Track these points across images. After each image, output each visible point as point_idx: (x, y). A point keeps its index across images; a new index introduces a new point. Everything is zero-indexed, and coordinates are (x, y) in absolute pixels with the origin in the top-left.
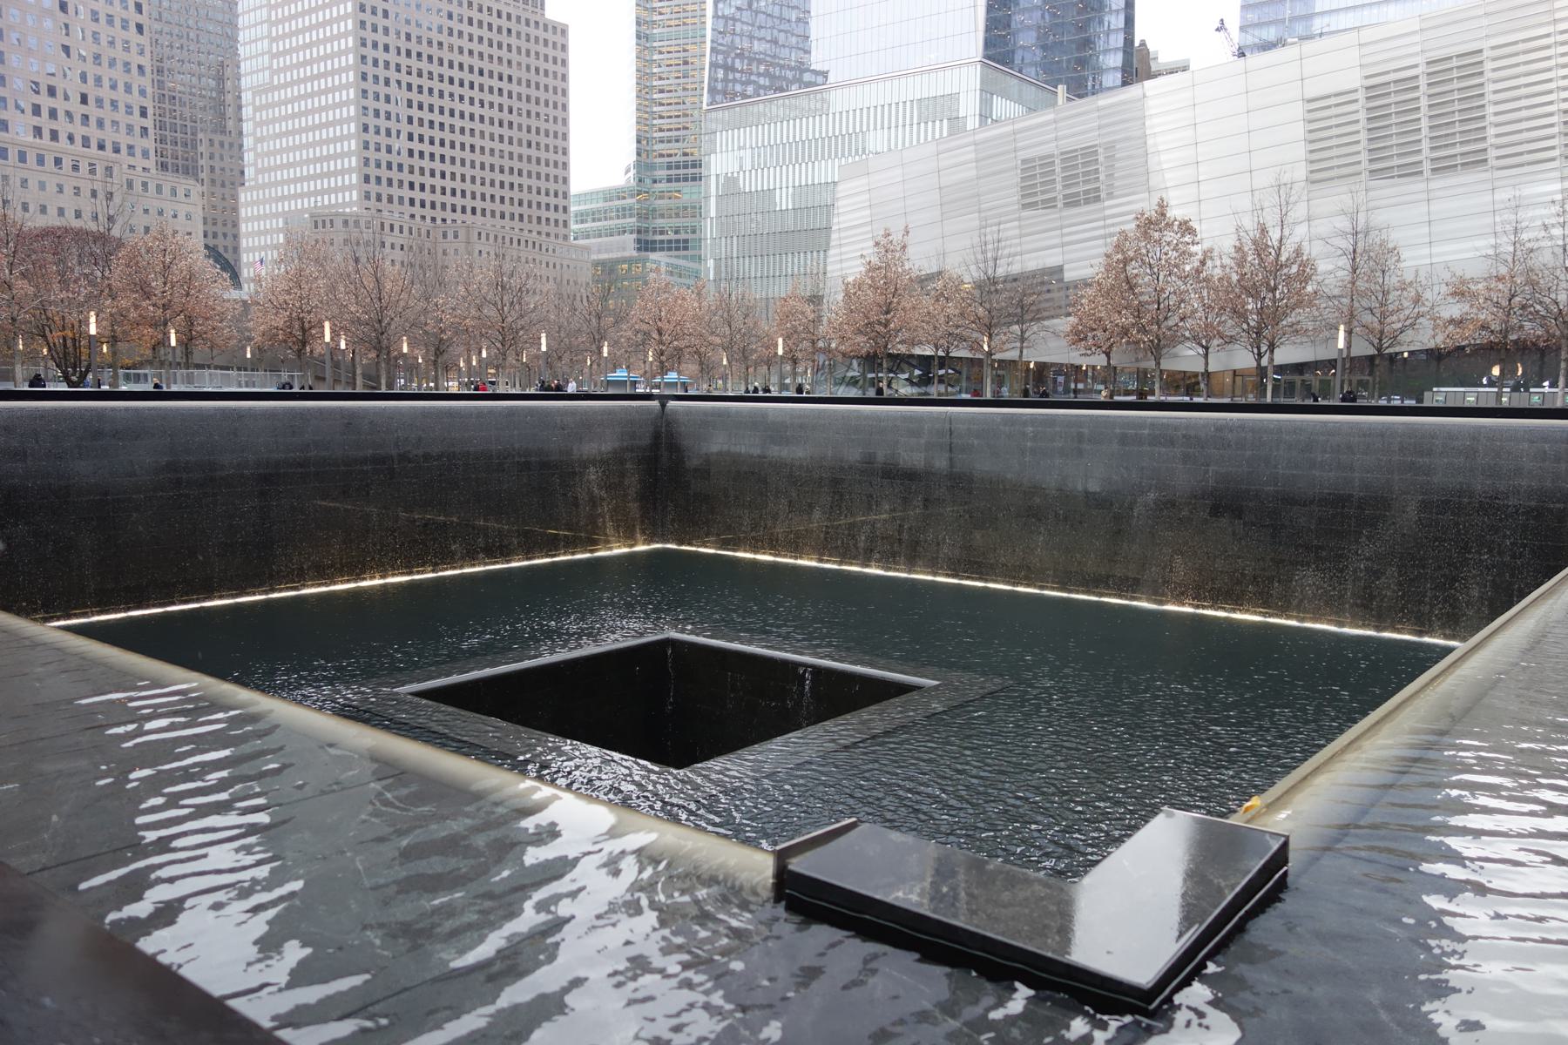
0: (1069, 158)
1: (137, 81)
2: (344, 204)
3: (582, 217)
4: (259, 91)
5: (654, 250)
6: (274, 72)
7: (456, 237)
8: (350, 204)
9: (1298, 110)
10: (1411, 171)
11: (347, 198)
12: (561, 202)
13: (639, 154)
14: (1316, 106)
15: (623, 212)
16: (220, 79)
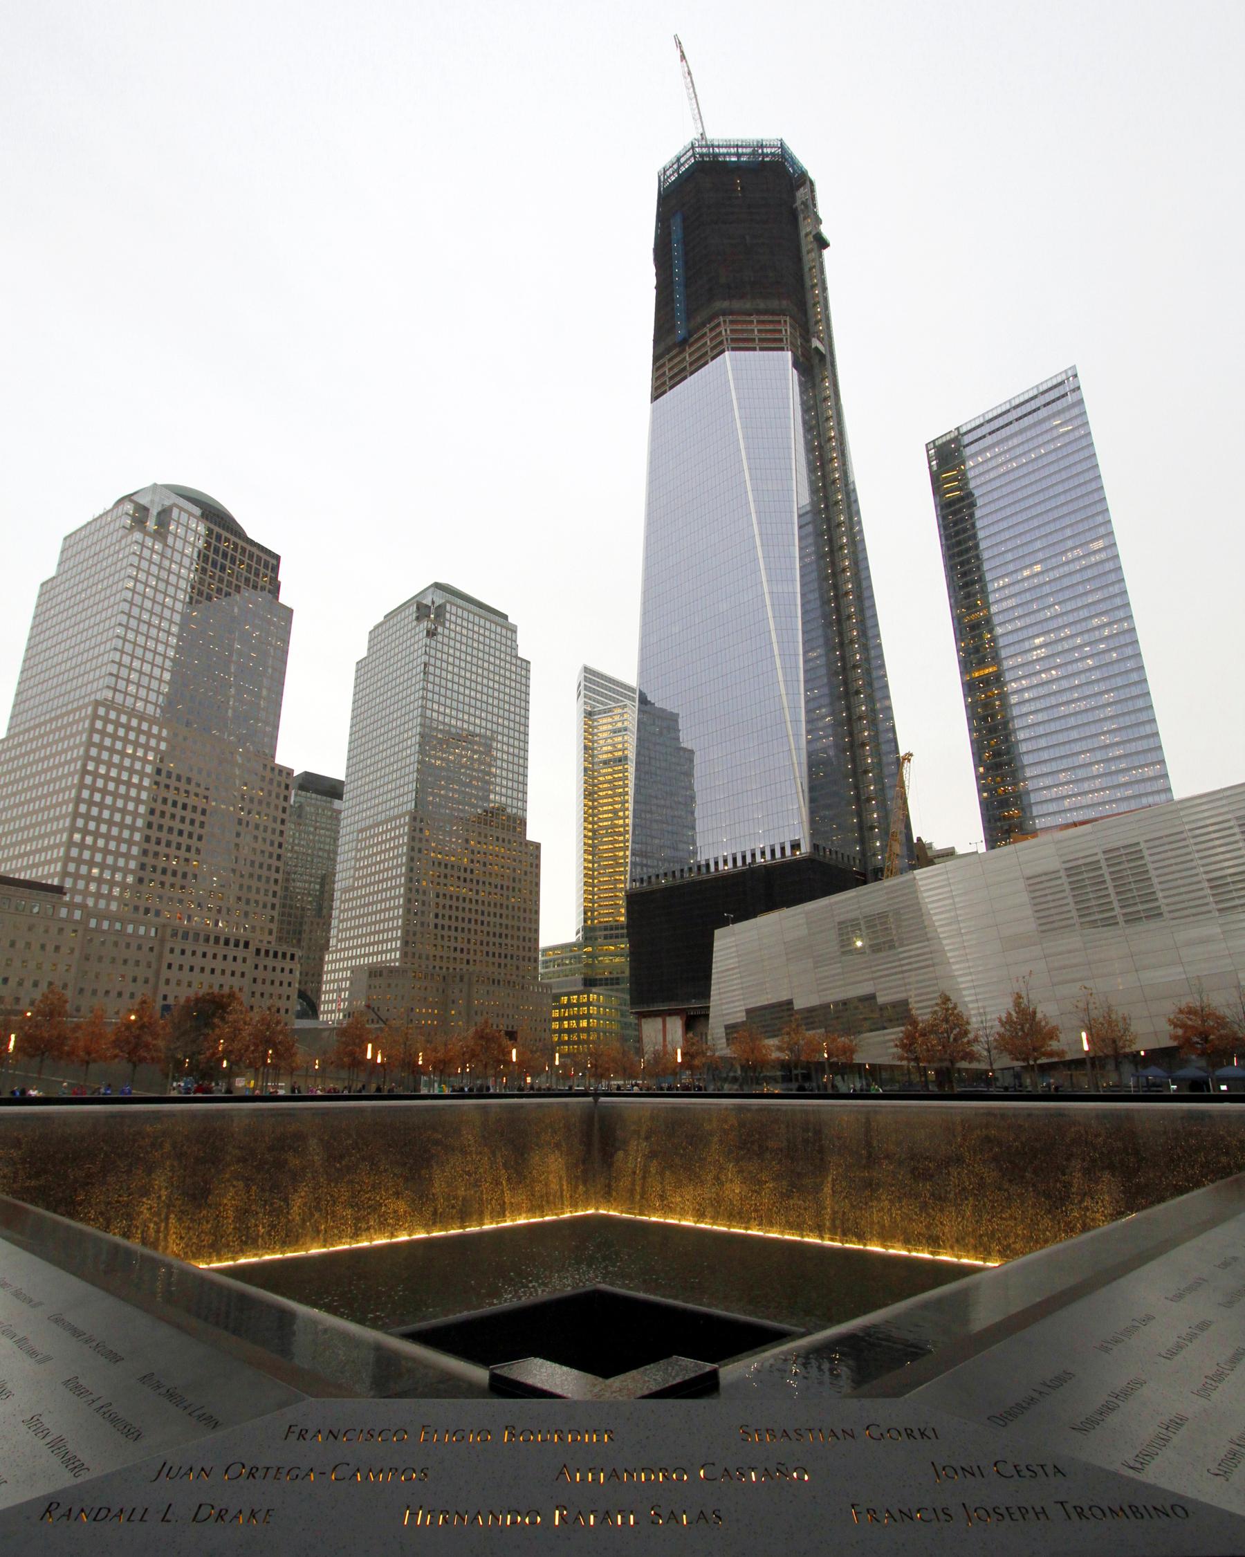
2: (391, 961)
4: (345, 891)
5: (595, 985)
6: (356, 879)
7: (462, 980)
8: (395, 960)
11: (393, 957)
12: (532, 954)
13: (585, 921)
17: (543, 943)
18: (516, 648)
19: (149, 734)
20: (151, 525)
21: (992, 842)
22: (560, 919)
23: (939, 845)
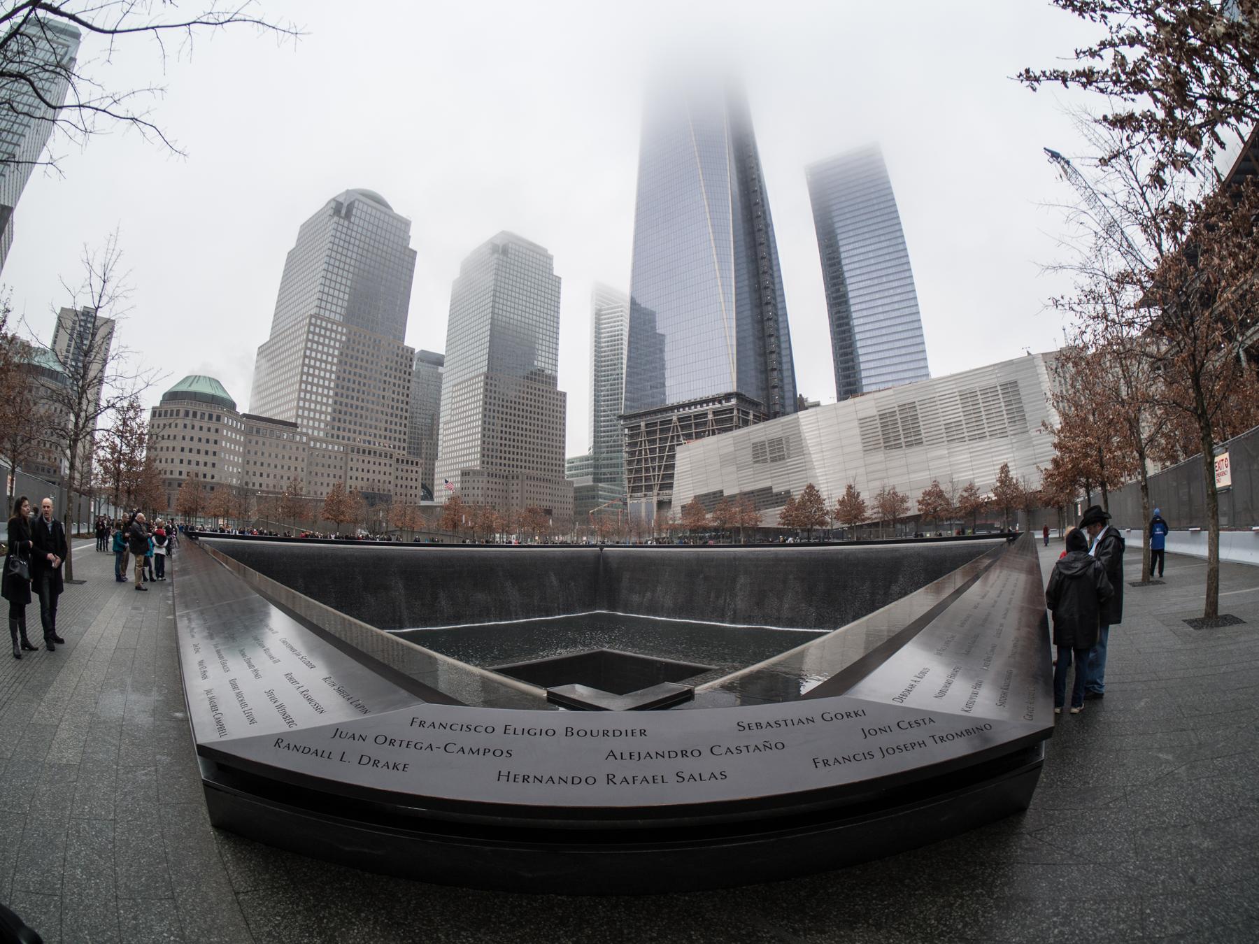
0: (771, 442)
1: (404, 422)
3: (570, 469)
4: (445, 423)
9: (856, 423)
10: (898, 446)
11: (476, 464)
14: (863, 422)
15: (587, 466)
16: (432, 419)
17: (568, 456)
18: (551, 269)
19: (336, 332)
20: (343, 212)
21: (840, 399)
22: (578, 440)
23: (811, 400)
